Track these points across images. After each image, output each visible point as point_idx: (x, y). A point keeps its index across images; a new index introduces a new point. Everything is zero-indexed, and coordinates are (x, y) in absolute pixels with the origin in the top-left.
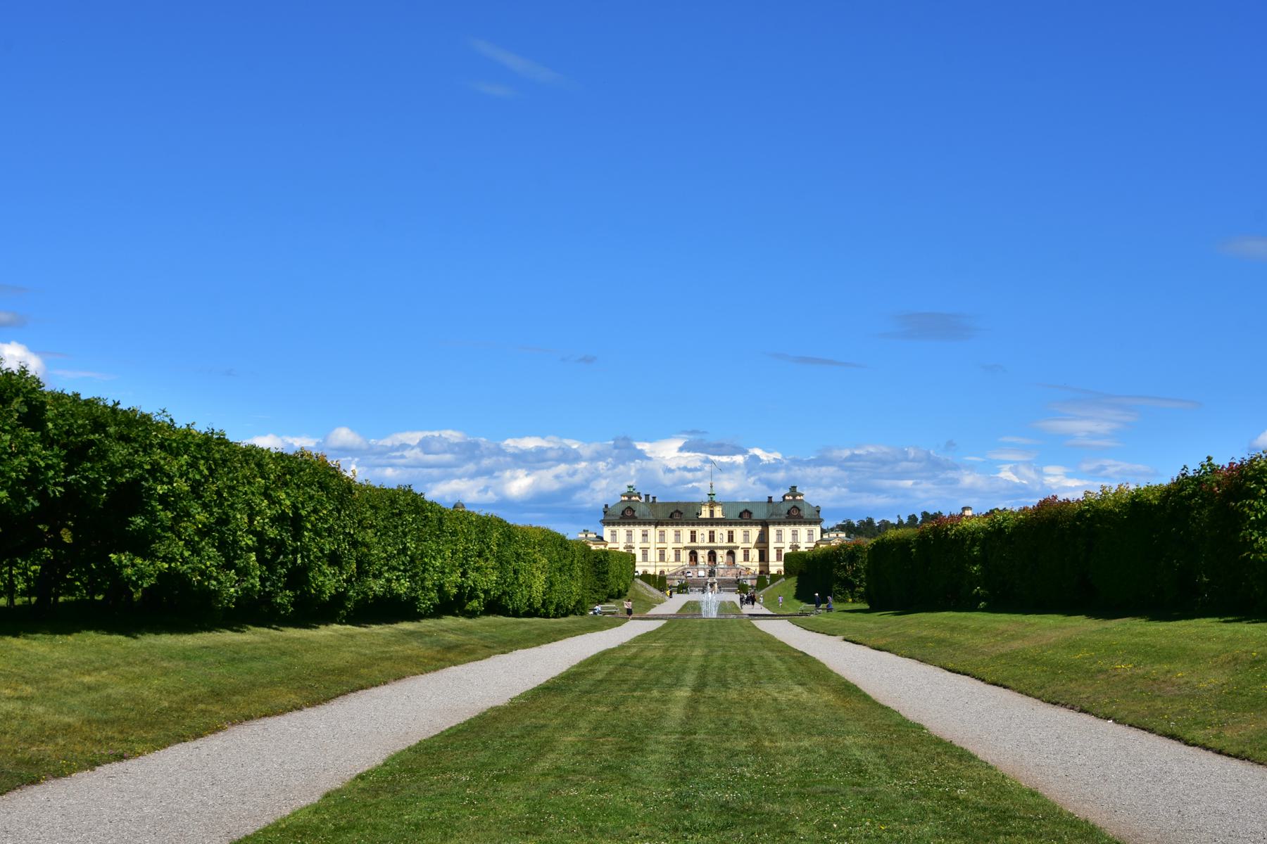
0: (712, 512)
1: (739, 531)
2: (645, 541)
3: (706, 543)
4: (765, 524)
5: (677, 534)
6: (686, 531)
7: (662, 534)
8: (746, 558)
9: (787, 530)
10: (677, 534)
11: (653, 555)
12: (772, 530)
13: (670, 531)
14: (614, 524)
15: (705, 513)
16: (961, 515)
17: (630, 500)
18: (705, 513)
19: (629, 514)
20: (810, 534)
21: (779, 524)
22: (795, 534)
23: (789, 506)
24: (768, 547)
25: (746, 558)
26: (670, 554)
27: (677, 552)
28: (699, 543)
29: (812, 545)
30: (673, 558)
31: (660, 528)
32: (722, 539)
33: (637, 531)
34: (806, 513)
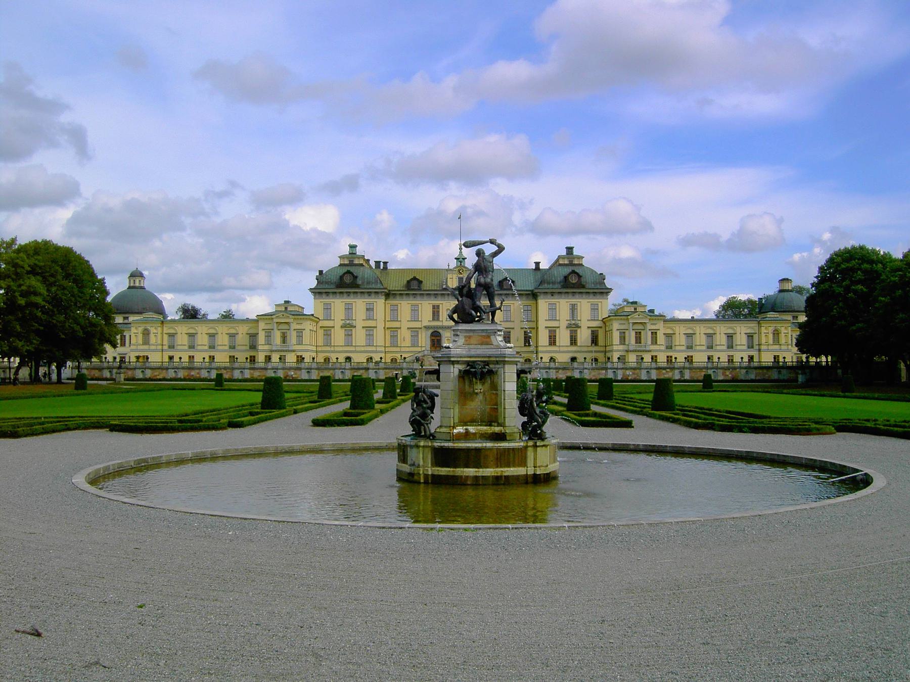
2: (369, 318)
4: (534, 295)
5: (415, 310)
6: (426, 306)
7: (394, 309)
9: (563, 304)
10: (415, 310)
11: (380, 337)
12: (543, 304)
13: (405, 306)
14: (327, 293)
16: (781, 291)
17: (351, 264)
19: (348, 279)
20: (594, 309)
21: (552, 294)
22: (573, 308)
23: (567, 271)
26: (405, 336)
27: (415, 332)
30: (408, 343)
31: (392, 302)
33: (359, 304)
34: (588, 279)
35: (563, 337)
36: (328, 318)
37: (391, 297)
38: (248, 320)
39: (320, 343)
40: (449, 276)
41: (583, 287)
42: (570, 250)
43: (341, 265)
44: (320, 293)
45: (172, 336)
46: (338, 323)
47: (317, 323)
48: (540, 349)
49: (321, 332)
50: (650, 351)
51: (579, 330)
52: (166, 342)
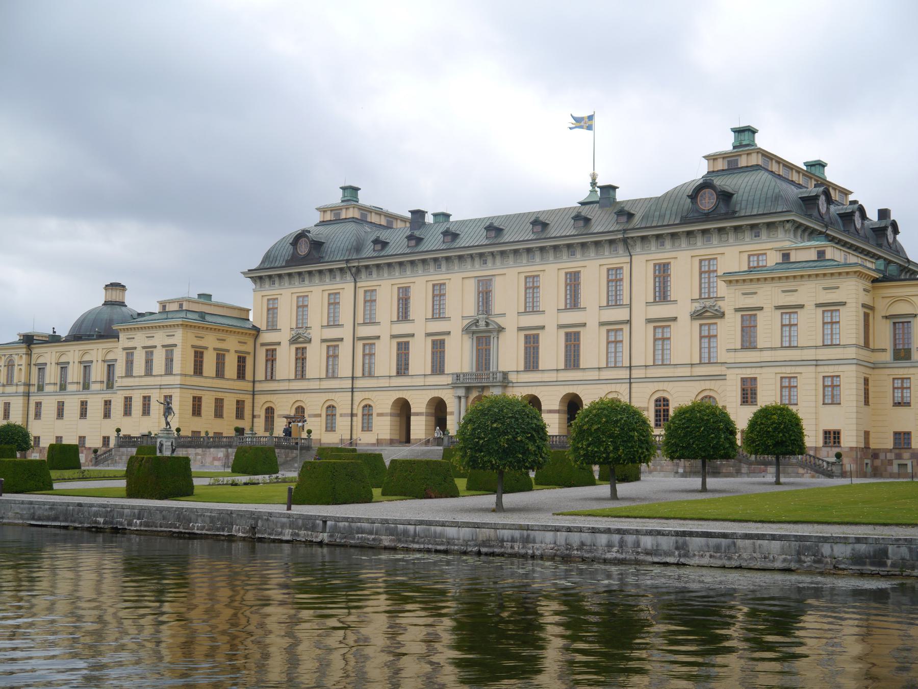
12: (641, 266)
22: (706, 271)
33: (317, 294)
35: (685, 340)
36: (272, 327)
37: (363, 275)
39: (260, 376)
41: (731, 215)
42: (745, 133)
43: (323, 223)
44: (260, 278)
45: (42, 368)
46: (283, 336)
47: (256, 337)
48: (636, 373)
52: (34, 380)
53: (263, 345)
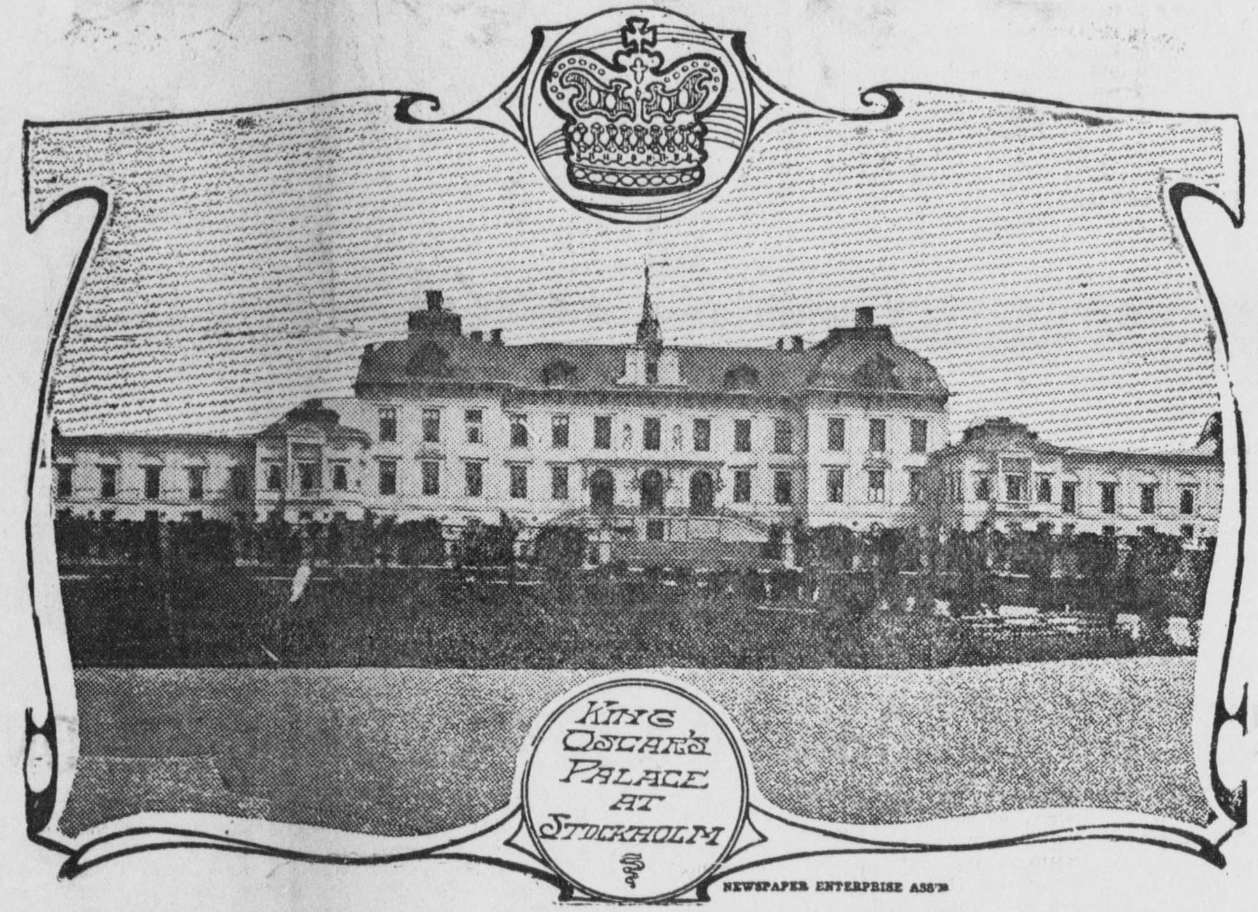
0: (652, 369)
1: (723, 423)
3: (637, 450)
4: (795, 404)
8: (743, 491)
12: (818, 421)
15: (635, 374)
18: (635, 374)
20: (919, 429)
24: (804, 467)
25: (743, 491)
26: (539, 480)
28: (618, 450)
29: (921, 460)
32: (677, 440)
33: (453, 414)
38: (222, 443)
40: (629, 358)
42: (866, 313)
49: (375, 468)
50: (1036, 514)
51: (887, 473)
53: (376, 457)
